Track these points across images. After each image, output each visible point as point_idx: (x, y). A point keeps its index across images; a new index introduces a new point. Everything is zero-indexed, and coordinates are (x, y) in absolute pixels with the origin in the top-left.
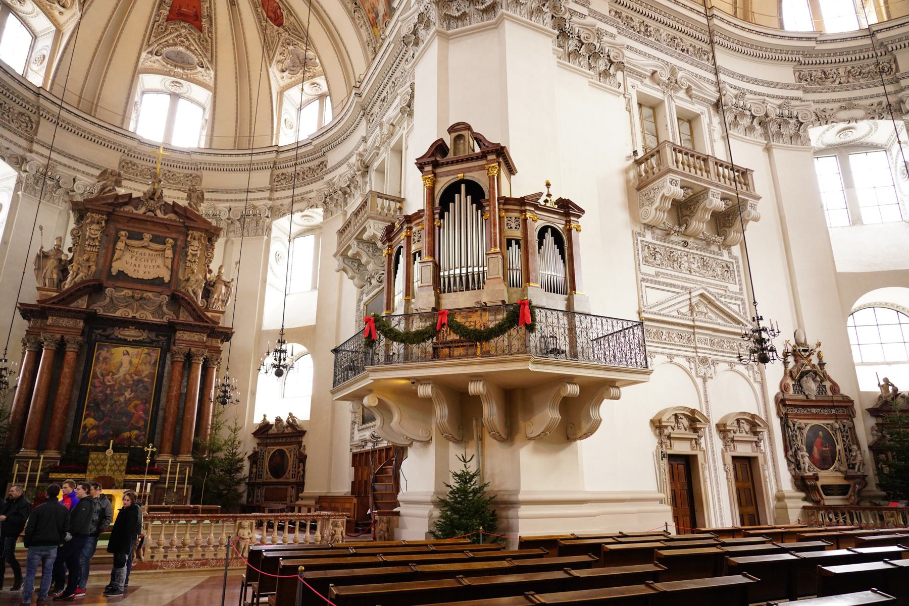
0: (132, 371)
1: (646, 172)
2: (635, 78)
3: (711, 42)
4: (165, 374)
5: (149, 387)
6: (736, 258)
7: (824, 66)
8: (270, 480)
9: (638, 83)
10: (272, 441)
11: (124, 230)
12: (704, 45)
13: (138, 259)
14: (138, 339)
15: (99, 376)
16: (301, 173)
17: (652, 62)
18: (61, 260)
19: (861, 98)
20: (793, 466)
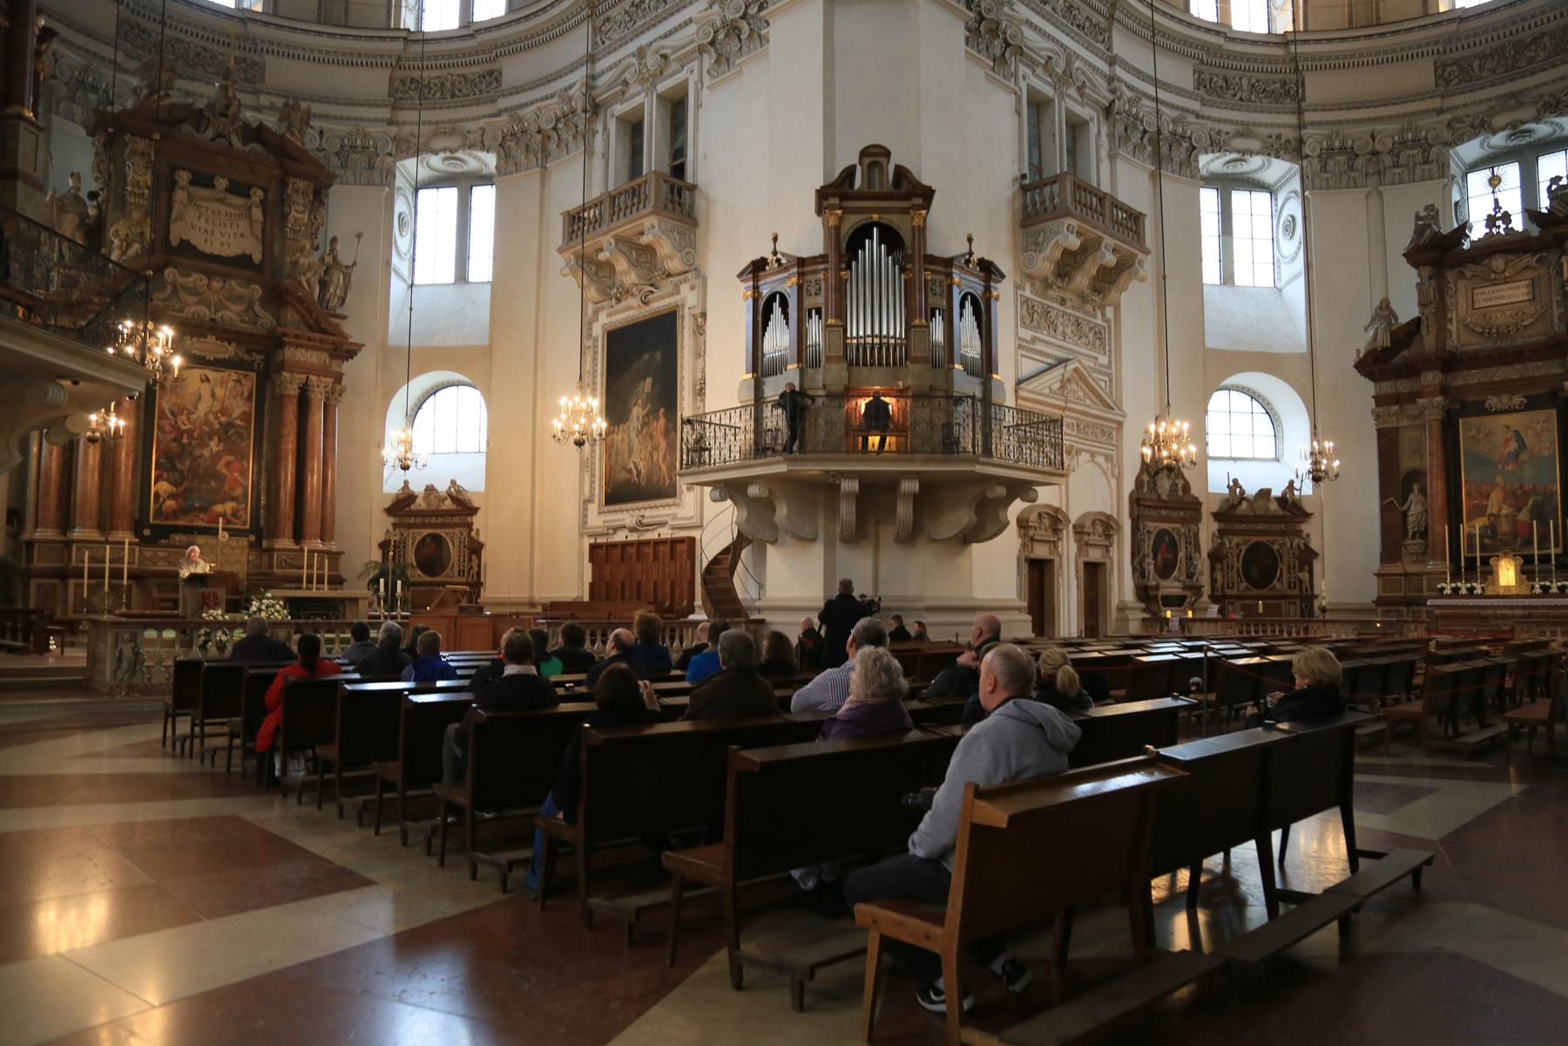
0: (217, 407)
1: (1034, 204)
2: (1026, 65)
3: (1112, 16)
4: (266, 415)
5: (246, 435)
6: (1108, 321)
7: (1228, 71)
8: (419, 579)
9: (1029, 72)
10: (419, 520)
11: (184, 169)
12: (1101, 19)
13: (210, 222)
14: (222, 356)
15: (169, 415)
16: (449, 86)
17: (1050, 45)
18: (83, 217)
19: (1260, 125)
20: (1137, 574)
